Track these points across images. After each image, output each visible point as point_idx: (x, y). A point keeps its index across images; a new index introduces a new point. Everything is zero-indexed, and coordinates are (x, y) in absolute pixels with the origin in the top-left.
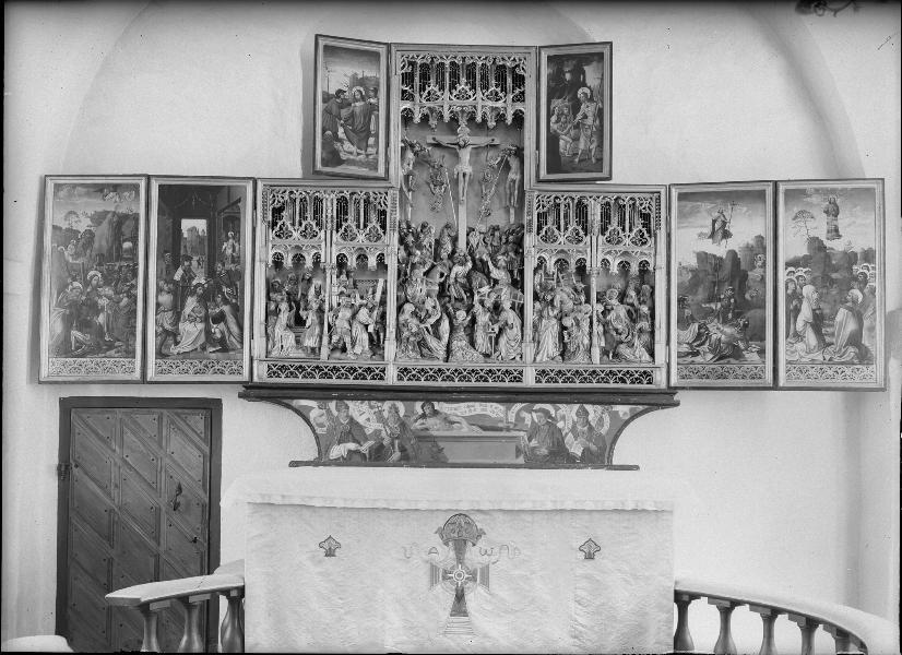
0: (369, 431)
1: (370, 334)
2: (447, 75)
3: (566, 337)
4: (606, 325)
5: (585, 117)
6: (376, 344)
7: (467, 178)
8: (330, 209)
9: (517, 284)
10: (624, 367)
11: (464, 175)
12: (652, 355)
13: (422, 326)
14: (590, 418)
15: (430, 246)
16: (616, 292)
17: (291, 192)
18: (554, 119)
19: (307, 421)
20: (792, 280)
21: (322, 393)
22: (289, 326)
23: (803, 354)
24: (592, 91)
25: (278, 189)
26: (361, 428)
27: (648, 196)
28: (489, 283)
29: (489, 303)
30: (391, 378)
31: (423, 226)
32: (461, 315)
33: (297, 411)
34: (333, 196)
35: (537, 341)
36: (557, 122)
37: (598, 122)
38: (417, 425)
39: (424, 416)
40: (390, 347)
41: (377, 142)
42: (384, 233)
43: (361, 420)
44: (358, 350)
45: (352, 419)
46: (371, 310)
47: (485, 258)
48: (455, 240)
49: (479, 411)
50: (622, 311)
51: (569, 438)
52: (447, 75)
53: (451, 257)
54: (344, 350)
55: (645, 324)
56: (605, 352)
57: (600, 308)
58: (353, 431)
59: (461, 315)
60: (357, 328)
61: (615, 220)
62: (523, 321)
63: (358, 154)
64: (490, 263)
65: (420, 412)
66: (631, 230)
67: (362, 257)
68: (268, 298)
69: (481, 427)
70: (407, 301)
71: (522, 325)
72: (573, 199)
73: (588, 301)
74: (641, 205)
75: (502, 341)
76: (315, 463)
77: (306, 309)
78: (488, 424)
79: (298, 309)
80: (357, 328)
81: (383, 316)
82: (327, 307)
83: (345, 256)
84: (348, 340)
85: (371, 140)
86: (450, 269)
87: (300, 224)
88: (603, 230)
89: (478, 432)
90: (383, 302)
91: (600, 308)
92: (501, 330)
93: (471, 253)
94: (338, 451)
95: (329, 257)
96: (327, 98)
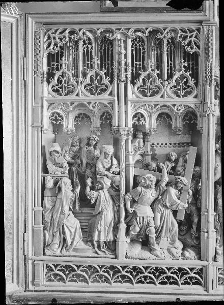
8: (124, 53)
17: (72, 33)
25: (54, 27)
77: (92, 188)
79: (84, 186)
83: (142, 116)
87: (85, 75)
90: (197, 178)
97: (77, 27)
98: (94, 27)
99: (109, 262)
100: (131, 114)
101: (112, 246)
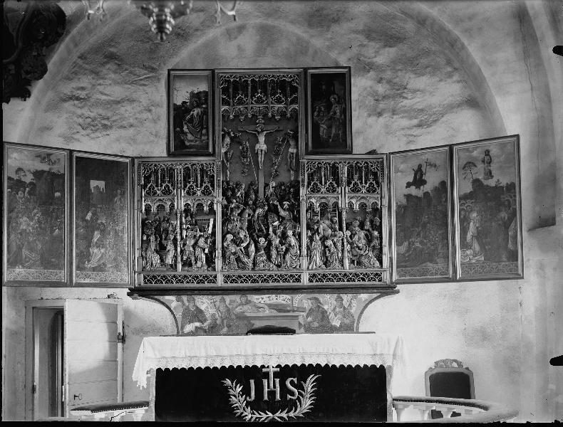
0: (208, 316)
1: (206, 254)
2: (250, 88)
3: (327, 252)
4: (351, 244)
5: (335, 113)
6: (210, 261)
7: (263, 152)
9: (297, 219)
10: (364, 270)
11: (262, 151)
12: (381, 263)
13: (239, 248)
14: (344, 302)
15: (242, 196)
16: (358, 223)
18: (316, 114)
19: (168, 308)
20: (463, 209)
21: (178, 292)
22: (157, 252)
23: (471, 257)
24: (339, 97)
26: (201, 311)
27: (375, 160)
28: (279, 220)
29: (279, 232)
30: (220, 282)
31: (237, 184)
32: (262, 240)
33: (163, 303)
34: (181, 167)
35: (310, 256)
36: (318, 116)
37: (343, 117)
38: (238, 310)
39: (241, 304)
40: (219, 263)
41: (208, 132)
42: (213, 190)
43: (203, 308)
44: (199, 264)
45: (197, 308)
46: (206, 239)
47: (276, 203)
48: (256, 192)
49: (275, 301)
50: (362, 234)
51: (332, 315)
52: (250, 88)
53: (254, 203)
54: (190, 265)
55: (376, 242)
56: (352, 262)
57: (349, 233)
58: (198, 315)
59: (262, 240)
60: (198, 251)
61: (356, 177)
62: (300, 243)
63: (196, 141)
64: (279, 207)
65: (239, 301)
66: (366, 183)
67: (200, 206)
68: (143, 233)
69: (277, 310)
70: (228, 233)
71: (300, 246)
72: (329, 164)
73: (341, 229)
74: (372, 166)
75: (288, 257)
76: (178, 335)
77: (166, 239)
78: (280, 307)
80: (198, 251)
81: (214, 242)
82: (179, 237)
83: (189, 205)
84: (193, 259)
85: (204, 131)
86: (254, 211)
87: (161, 186)
88: (349, 183)
89: (275, 313)
90: (214, 234)
91: (349, 233)
92: (287, 250)
93: (267, 200)
94: (189, 328)
95: (181, 204)
96: (177, 108)
97: (157, 163)
98: (166, 163)
99: (173, 273)
100: (183, 204)
101: (174, 267)
